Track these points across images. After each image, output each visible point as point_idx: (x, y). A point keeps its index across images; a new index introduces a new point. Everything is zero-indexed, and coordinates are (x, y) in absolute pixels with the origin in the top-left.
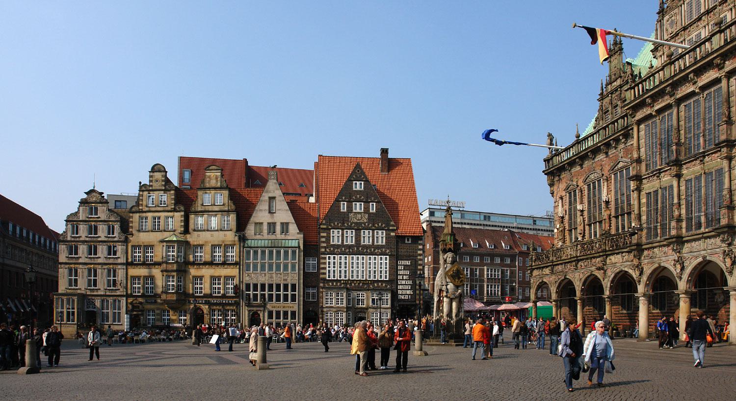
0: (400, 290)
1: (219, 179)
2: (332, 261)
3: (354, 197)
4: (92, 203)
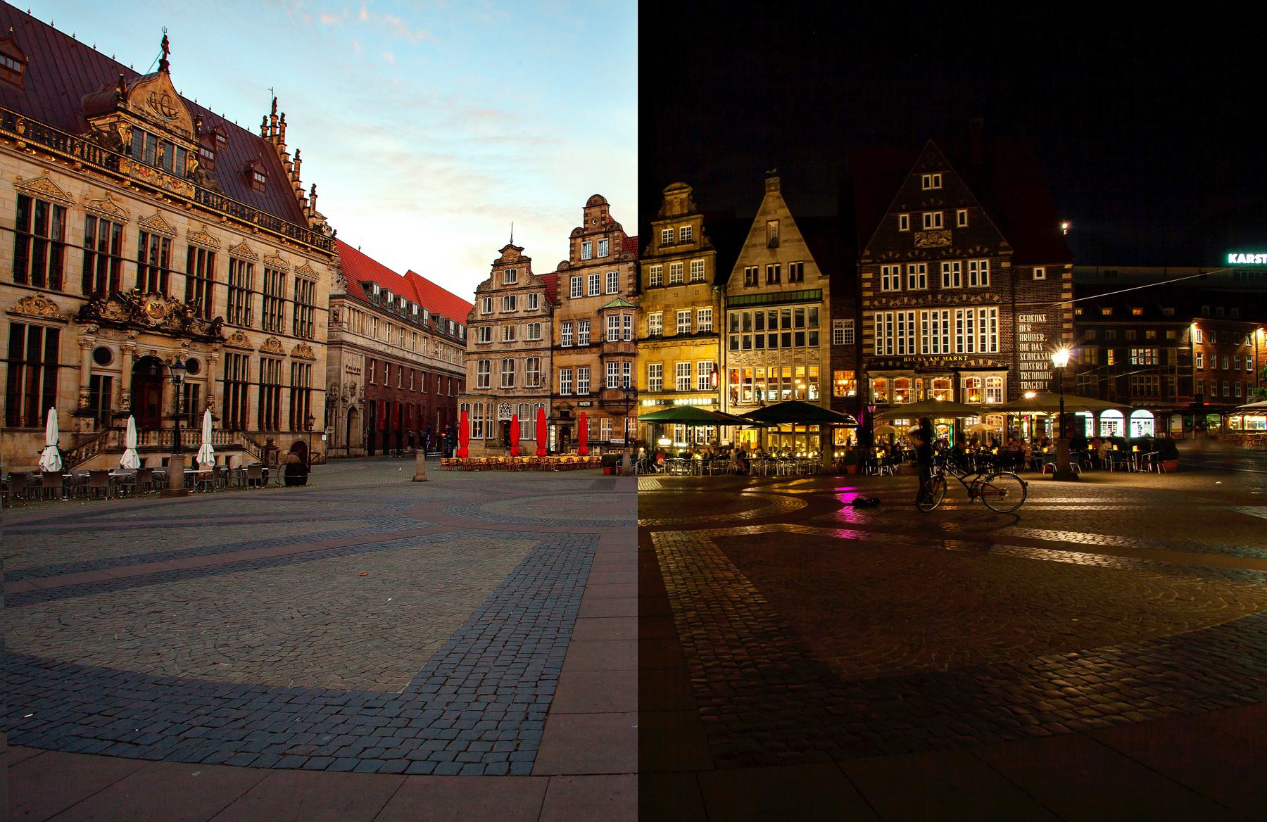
0: (1024, 371)
1: (686, 203)
3: (924, 204)
4: (508, 264)
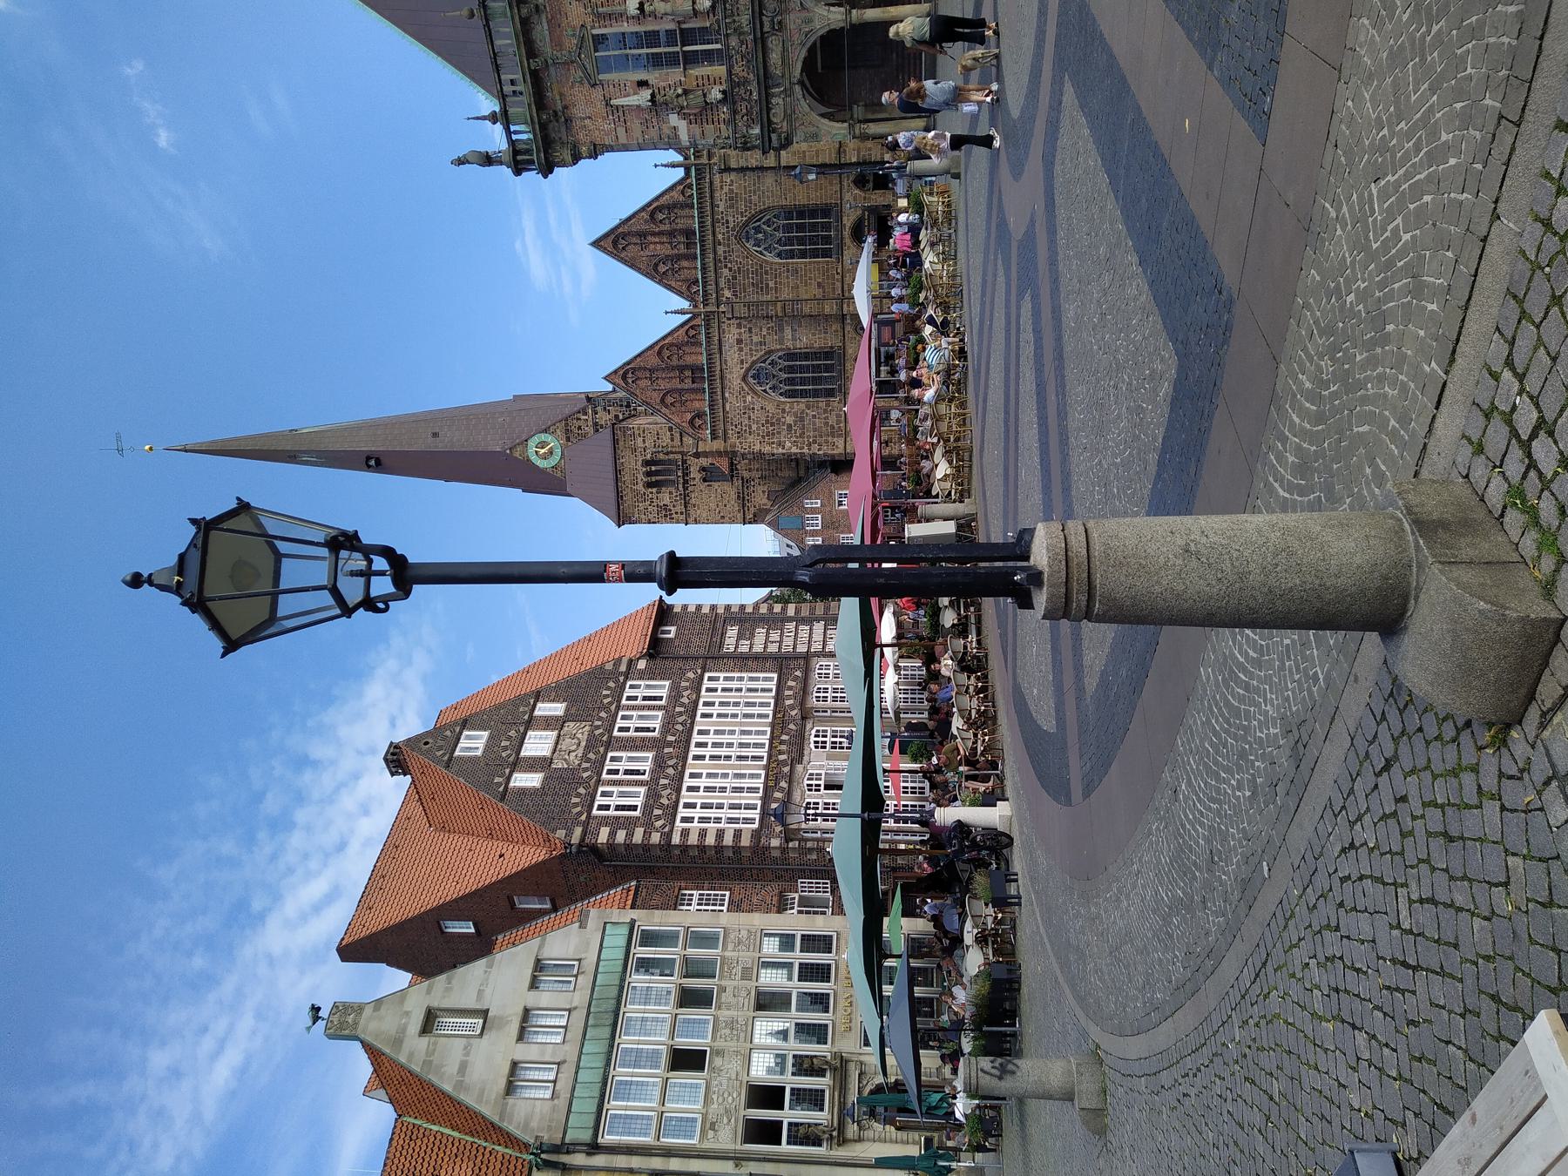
2: (697, 813)
